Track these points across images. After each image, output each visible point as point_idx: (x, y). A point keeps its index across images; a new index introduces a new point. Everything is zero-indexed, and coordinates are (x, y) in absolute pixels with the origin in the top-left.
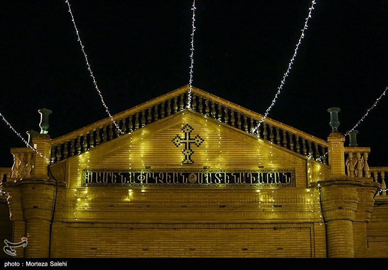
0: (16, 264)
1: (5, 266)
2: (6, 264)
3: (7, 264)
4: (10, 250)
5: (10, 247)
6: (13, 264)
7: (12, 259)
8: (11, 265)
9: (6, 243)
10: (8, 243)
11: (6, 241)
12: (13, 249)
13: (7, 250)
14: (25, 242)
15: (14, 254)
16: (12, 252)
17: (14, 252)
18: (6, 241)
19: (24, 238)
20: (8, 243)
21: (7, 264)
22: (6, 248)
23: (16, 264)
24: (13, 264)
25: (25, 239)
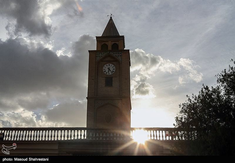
0: (10, 160)
1: (3, 160)
2: (4, 160)
3: (4, 160)
4: (6, 151)
5: (5, 149)
6: (8, 160)
7: (7, 157)
8: (7, 160)
9: (3, 147)
10: (5, 147)
11: (3, 146)
12: (7, 150)
13: (4, 151)
14: (15, 146)
15: (8, 153)
16: (7, 152)
17: (8, 152)
18: (3, 146)
19: (14, 144)
20: (5, 147)
21: (4, 160)
22: (3, 150)
23: (10, 160)
24: (8, 160)
25: (15, 145)
